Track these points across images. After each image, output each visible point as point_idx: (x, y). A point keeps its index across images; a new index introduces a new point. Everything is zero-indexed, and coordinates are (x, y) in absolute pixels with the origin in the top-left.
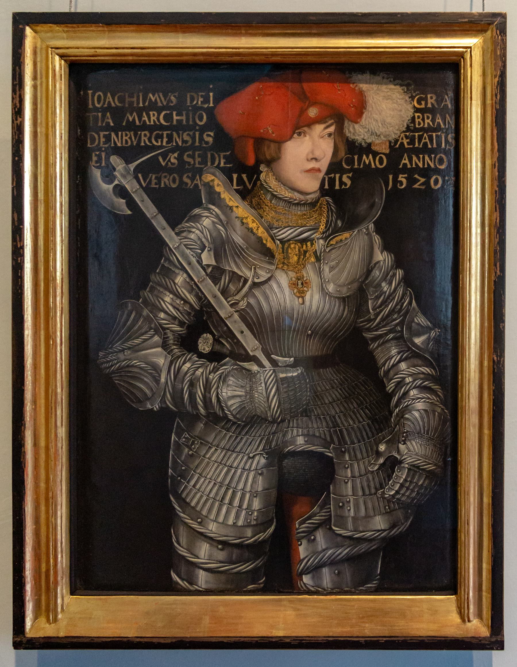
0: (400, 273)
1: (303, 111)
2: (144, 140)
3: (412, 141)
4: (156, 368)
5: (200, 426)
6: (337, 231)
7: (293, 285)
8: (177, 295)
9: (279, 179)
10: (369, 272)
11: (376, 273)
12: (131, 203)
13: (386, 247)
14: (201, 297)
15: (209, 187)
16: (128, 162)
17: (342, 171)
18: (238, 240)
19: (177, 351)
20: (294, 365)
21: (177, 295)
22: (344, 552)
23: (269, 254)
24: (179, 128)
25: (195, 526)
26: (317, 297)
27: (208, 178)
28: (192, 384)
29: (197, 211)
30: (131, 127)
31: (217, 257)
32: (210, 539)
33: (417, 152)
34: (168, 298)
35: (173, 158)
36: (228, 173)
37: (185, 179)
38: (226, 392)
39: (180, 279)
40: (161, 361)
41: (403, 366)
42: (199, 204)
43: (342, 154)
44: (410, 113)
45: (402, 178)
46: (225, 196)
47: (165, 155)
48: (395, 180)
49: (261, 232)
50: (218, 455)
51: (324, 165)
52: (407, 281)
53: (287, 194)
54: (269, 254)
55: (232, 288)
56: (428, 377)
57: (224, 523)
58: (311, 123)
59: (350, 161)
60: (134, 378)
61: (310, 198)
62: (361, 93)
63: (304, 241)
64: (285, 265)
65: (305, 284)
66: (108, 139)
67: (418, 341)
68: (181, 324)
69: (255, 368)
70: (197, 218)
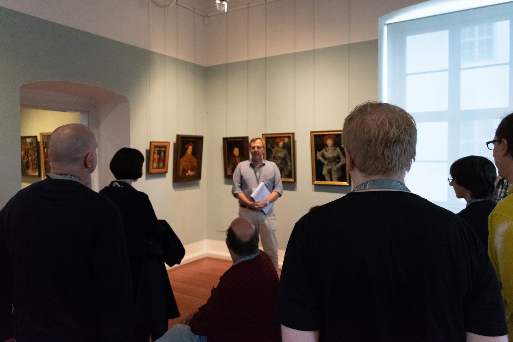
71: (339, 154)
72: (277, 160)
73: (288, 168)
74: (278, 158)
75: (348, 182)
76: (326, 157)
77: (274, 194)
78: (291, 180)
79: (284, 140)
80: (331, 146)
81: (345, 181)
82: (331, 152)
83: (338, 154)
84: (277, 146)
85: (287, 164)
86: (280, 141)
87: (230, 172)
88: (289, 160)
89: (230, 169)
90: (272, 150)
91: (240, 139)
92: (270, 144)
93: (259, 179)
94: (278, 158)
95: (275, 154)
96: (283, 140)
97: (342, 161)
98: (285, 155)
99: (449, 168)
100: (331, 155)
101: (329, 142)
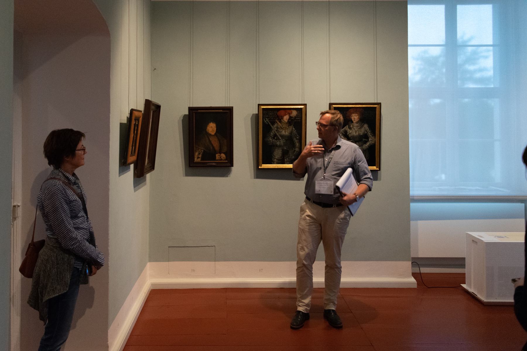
0: (295, 131)
5: (275, 147)
9: (283, 120)
10: (292, 130)
11: (293, 130)
12: (268, 123)
13: (294, 128)
14: (275, 133)
15: (276, 121)
16: (268, 118)
18: (279, 127)
32: (276, 159)
35: (272, 118)
36: (278, 120)
39: (273, 131)
40: (271, 140)
42: (275, 123)
51: (288, 119)
53: (284, 122)
54: (282, 128)
58: (287, 114)
62: (292, 111)
67: (297, 138)
70: (275, 125)
71: (367, 131)
72: (279, 139)
73: (295, 151)
74: (280, 138)
75: (377, 166)
76: (350, 136)
77: (363, 187)
79: (292, 113)
80: (357, 123)
82: (356, 130)
83: (366, 132)
84: (280, 122)
85: (294, 145)
86: (285, 115)
87: (198, 158)
88: (297, 139)
89: (199, 154)
90: (272, 126)
91: (221, 111)
93: (327, 167)
94: (280, 138)
95: (276, 132)
96: (289, 114)
97: (371, 140)
98: (291, 133)
99: (42, 149)
100: (356, 133)
101: (355, 117)
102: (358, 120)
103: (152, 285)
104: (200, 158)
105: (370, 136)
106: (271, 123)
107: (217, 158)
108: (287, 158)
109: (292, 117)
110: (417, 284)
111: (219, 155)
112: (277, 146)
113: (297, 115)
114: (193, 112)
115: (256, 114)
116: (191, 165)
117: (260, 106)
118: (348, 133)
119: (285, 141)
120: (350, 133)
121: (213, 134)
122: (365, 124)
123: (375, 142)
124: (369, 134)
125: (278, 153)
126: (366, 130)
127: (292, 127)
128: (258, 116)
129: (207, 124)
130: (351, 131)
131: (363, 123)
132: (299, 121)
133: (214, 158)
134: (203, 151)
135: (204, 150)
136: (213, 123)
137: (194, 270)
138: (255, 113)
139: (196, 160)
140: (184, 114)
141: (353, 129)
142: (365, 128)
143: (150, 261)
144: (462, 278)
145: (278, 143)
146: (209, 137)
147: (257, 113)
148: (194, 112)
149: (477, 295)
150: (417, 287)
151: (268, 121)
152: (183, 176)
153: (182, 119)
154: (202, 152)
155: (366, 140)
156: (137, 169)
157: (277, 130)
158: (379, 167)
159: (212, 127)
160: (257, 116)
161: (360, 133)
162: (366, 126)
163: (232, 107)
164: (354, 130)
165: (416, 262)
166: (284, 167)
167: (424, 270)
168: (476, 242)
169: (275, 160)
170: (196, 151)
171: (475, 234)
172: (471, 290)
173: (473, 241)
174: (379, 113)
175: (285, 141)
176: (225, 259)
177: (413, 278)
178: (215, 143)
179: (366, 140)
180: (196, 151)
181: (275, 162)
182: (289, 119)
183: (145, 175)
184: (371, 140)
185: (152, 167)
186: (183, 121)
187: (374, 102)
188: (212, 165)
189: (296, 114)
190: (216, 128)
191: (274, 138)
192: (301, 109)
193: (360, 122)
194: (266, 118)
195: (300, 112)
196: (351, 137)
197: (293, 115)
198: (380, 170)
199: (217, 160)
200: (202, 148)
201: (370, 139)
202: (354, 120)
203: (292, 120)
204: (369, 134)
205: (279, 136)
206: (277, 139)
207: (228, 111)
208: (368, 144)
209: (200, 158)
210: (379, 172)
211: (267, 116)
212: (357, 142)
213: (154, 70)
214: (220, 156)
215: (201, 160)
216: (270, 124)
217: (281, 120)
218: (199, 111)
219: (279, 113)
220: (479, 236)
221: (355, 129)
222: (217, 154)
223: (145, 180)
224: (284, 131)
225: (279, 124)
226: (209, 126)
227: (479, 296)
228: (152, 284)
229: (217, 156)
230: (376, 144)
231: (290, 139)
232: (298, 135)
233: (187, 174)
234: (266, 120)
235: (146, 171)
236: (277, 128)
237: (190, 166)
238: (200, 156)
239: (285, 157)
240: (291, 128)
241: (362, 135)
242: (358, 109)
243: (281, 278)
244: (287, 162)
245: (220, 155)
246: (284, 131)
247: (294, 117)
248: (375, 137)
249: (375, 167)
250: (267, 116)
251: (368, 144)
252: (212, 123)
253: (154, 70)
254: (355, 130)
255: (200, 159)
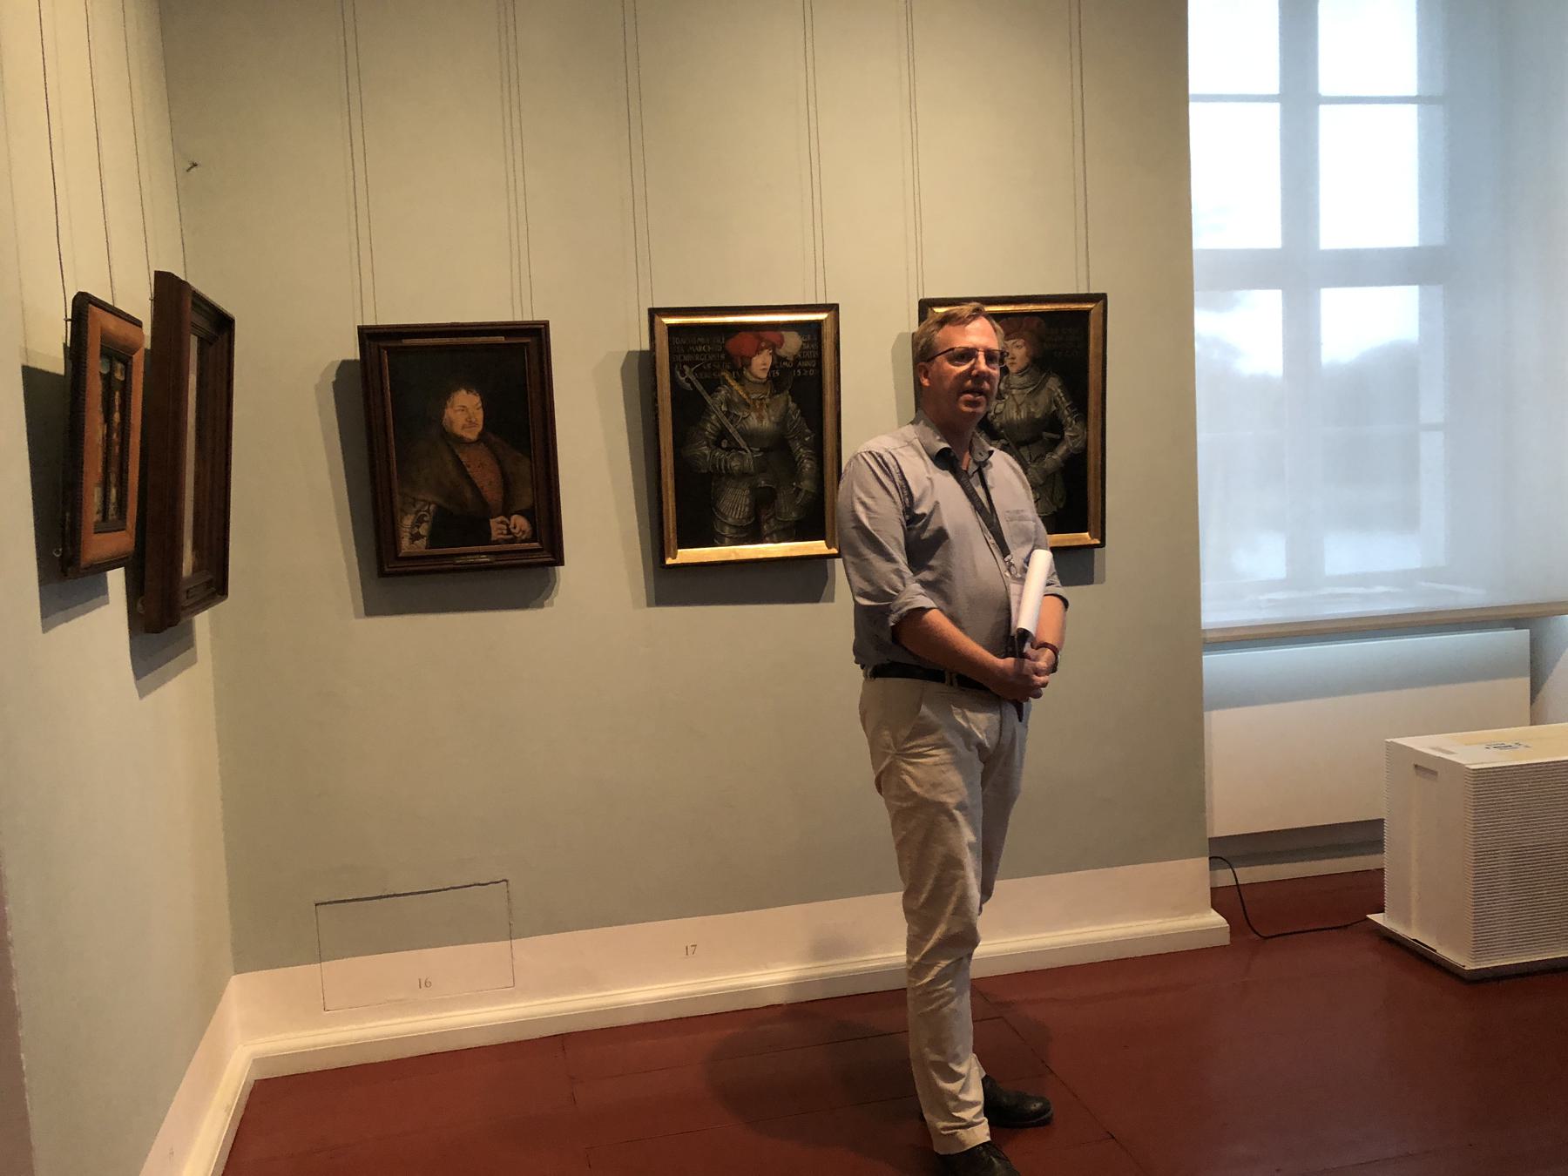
0: (799, 411)
1: (759, 344)
2: (697, 358)
3: (802, 355)
4: (705, 455)
5: (723, 478)
6: (774, 394)
7: (758, 418)
8: (712, 423)
10: (787, 411)
11: (790, 412)
14: (722, 424)
15: (723, 376)
17: (776, 369)
18: (736, 400)
19: (713, 447)
20: (759, 452)
21: (712, 423)
22: (782, 527)
23: (748, 405)
24: (711, 352)
25: (723, 519)
26: (768, 422)
27: (723, 374)
28: (720, 460)
29: (719, 388)
30: (691, 352)
31: (728, 406)
32: (730, 525)
33: (804, 360)
34: (709, 425)
35: (709, 365)
36: (730, 371)
37: (714, 374)
38: (733, 464)
39: (713, 417)
40: (707, 452)
41: (801, 450)
42: (720, 385)
43: (776, 362)
44: (801, 343)
45: (799, 371)
46: (730, 381)
47: (706, 364)
48: (797, 373)
49: (745, 396)
50: (731, 490)
51: (768, 367)
52: (802, 414)
53: (753, 379)
54: (748, 405)
55: (735, 420)
56: (812, 454)
57: (734, 518)
58: (763, 349)
59: (779, 365)
60: (698, 459)
61: (764, 381)
62: (782, 337)
63: (761, 399)
64: (755, 410)
65: (763, 417)
66: (682, 358)
67: (807, 439)
68: (714, 436)
69: (744, 453)
70: (720, 391)
74: (742, 443)
76: (997, 423)
78: (1085, 538)
79: (782, 342)
80: (1021, 372)
81: (1083, 528)
83: (1054, 408)
84: (740, 379)
85: (794, 471)
86: (758, 351)
87: (415, 537)
88: (804, 445)
89: (419, 521)
90: (708, 398)
91: (501, 339)
92: (690, 364)
94: (742, 443)
95: (725, 421)
96: (774, 347)
98: (783, 422)
100: (1018, 412)
102: (1027, 360)
103: (257, 1062)
104: (423, 537)
105: (1069, 419)
106: (702, 385)
107: (495, 535)
108: (769, 519)
109: (785, 359)
110: (1228, 930)
111: (502, 522)
112: (730, 474)
113: (802, 350)
114: (379, 347)
115: (642, 352)
116: (387, 570)
117: (657, 318)
118: (992, 414)
119: (760, 455)
120: (997, 411)
121: (472, 435)
122: (1051, 378)
123: (1087, 445)
124: (1067, 415)
125: (735, 503)
126: (1055, 401)
127: (785, 398)
128: (655, 357)
129: (444, 396)
130: (1001, 406)
131: (1041, 375)
132: (812, 372)
133: (485, 539)
134: (432, 507)
135: (439, 507)
136: (468, 391)
137: (428, 984)
138: (639, 349)
139: (405, 545)
140: (340, 360)
141: (1007, 397)
142: (1050, 390)
143: (237, 972)
144: (1370, 891)
145: (735, 464)
146: (457, 451)
147: (646, 346)
148: (385, 348)
149: (1435, 951)
150: (1231, 941)
151: (692, 378)
152: (357, 616)
153: (334, 379)
154: (428, 511)
155: (1054, 436)
156: (142, 595)
157: (727, 414)
158: (1100, 535)
159: (464, 409)
160: (644, 364)
161: (1034, 413)
162: (1053, 384)
163: (546, 324)
164: (1014, 403)
165: (1225, 852)
166: (761, 556)
167: (1249, 874)
168: (1434, 773)
169: (727, 528)
170: (402, 510)
171: (1423, 744)
172: (1410, 932)
173: (1416, 766)
174: (1100, 332)
175: (760, 455)
176: (552, 924)
177: (1214, 912)
178: (485, 476)
179: (1054, 436)
180: (402, 510)
181: (725, 536)
182: (773, 368)
183: (184, 620)
184: (1072, 434)
185: (216, 586)
186: (337, 386)
187: (1075, 292)
188: (471, 563)
189: (799, 347)
190: (484, 410)
191: (718, 444)
192: (819, 323)
193: (1032, 370)
194: (684, 367)
195: (812, 337)
196: (1001, 428)
197: (789, 350)
198: (1103, 544)
199: (497, 542)
200: (430, 499)
201: (1066, 434)
202: (1013, 363)
203: (784, 371)
204: (1066, 412)
205: (737, 436)
206: (728, 449)
207: (529, 340)
208: (1061, 450)
209: (423, 537)
210: (1096, 550)
211: (686, 358)
212: (1023, 446)
213: (188, 171)
214: (508, 525)
215: (430, 546)
216: (700, 387)
217: (741, 371)
218: (407, 342)
219: (733, 345)
220: (1433, 749)
221: (1017, 398)
222: (492, 518)
223: (188, 641)
224: (753, 415)
225: (736, 386)
226: (452, 406)
227: (1445, 952)
228: (254, 1061)
229: (496, 526)
230: (1091, 449)
231: (777, 447)
232: (807, 431)
233: (373, 607)
234: (683, 373)
235: (191, 601)
236: (729, 403)
237: (382, 574)
238: (423, 530)
239: (764, 517)
240: (782, 404)
241: (1039, 420)
242: (1026, 318)
243: (767, 968)
244: (770, 535)
245: (505, 519)
246: (753, 415)
247: (792, 359)
248: (1086, 425)
249: (1087, 534)
250: (686, 358)
251: (1061, 450)
252: (464, 392)
253: (188, 171)
254: (1014, 400)
255: (422, 543)
